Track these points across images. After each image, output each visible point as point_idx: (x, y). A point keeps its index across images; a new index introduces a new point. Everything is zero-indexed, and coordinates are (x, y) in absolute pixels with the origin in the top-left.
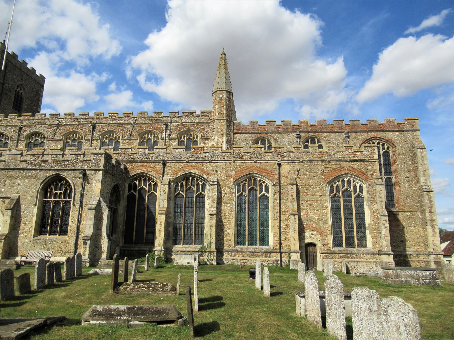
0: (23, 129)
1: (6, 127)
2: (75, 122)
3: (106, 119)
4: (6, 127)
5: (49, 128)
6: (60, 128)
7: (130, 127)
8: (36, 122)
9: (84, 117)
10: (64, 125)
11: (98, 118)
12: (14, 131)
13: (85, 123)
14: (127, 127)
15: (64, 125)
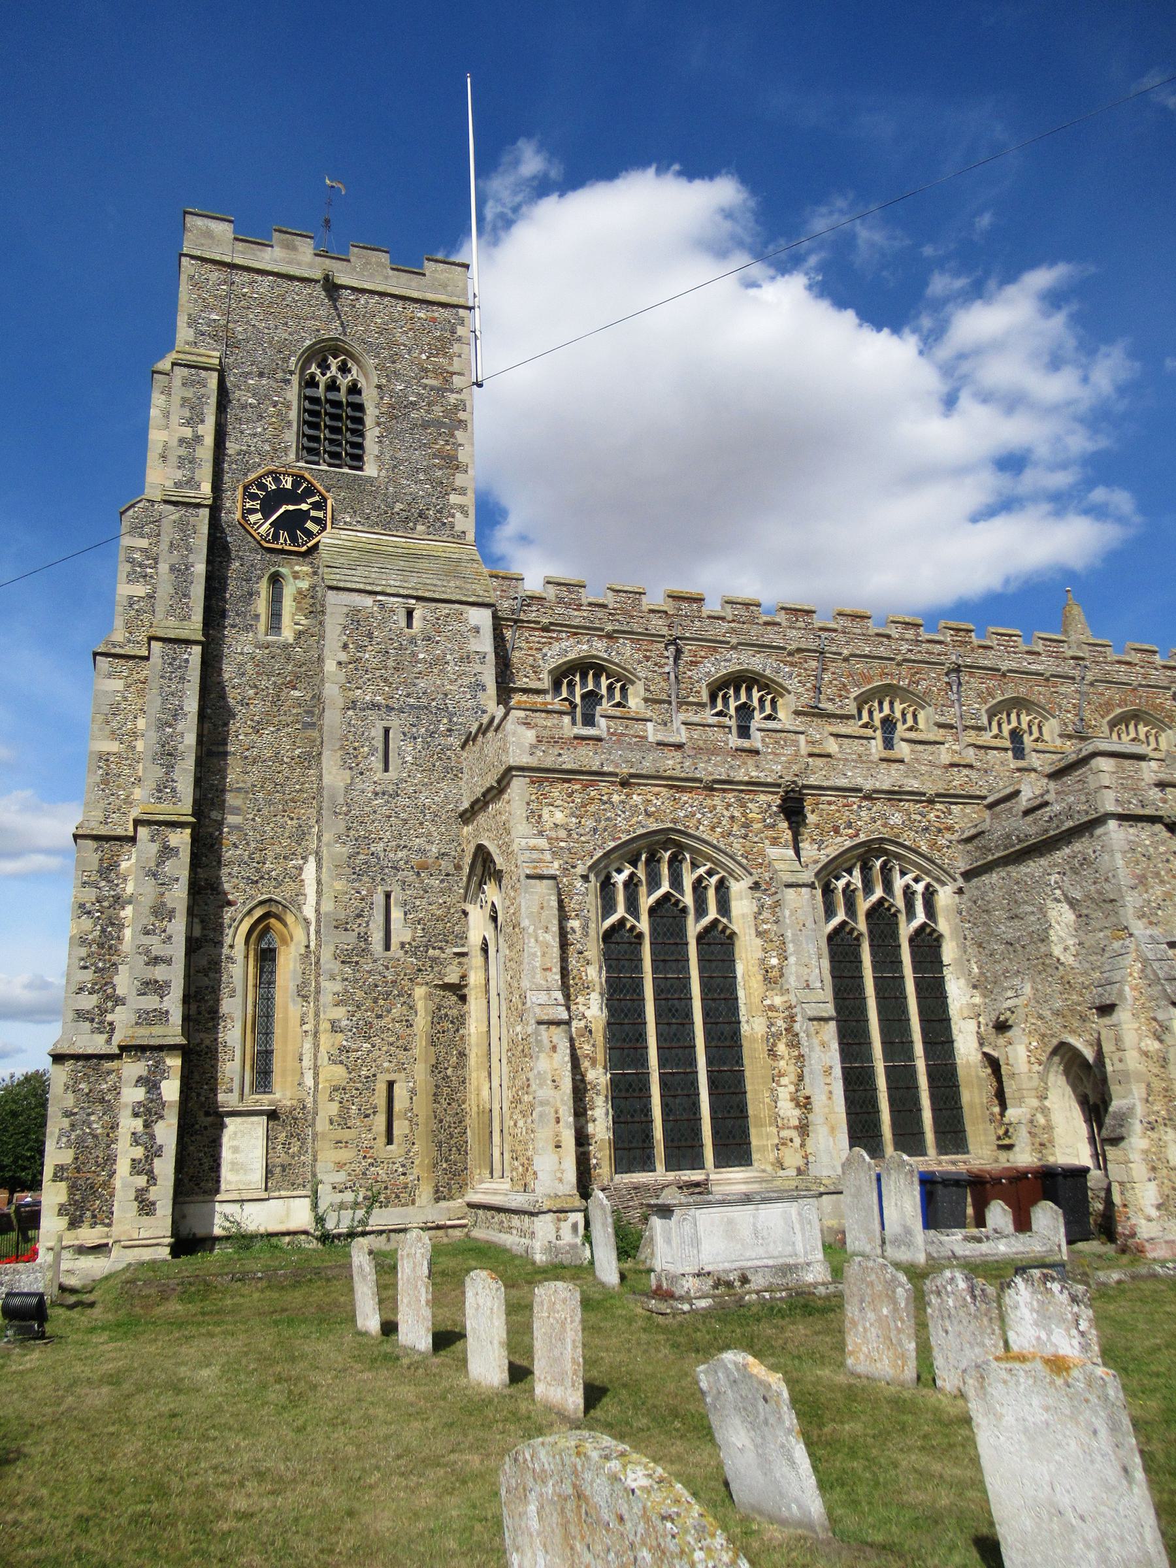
0: (686, 657)
1: (609, 636)
2: (882, 651)
3: (991, 653)
4: (609, 636)
5: (792, 664)
6: (832, 667)
7: (1068, 689)
8: (733, 631)
9: (910, 634)
10: (846, 660)
11: (964, 643)
12: (648, 658)
13: (919, 657)
14: (1062, 689)
15: (846, 660)
